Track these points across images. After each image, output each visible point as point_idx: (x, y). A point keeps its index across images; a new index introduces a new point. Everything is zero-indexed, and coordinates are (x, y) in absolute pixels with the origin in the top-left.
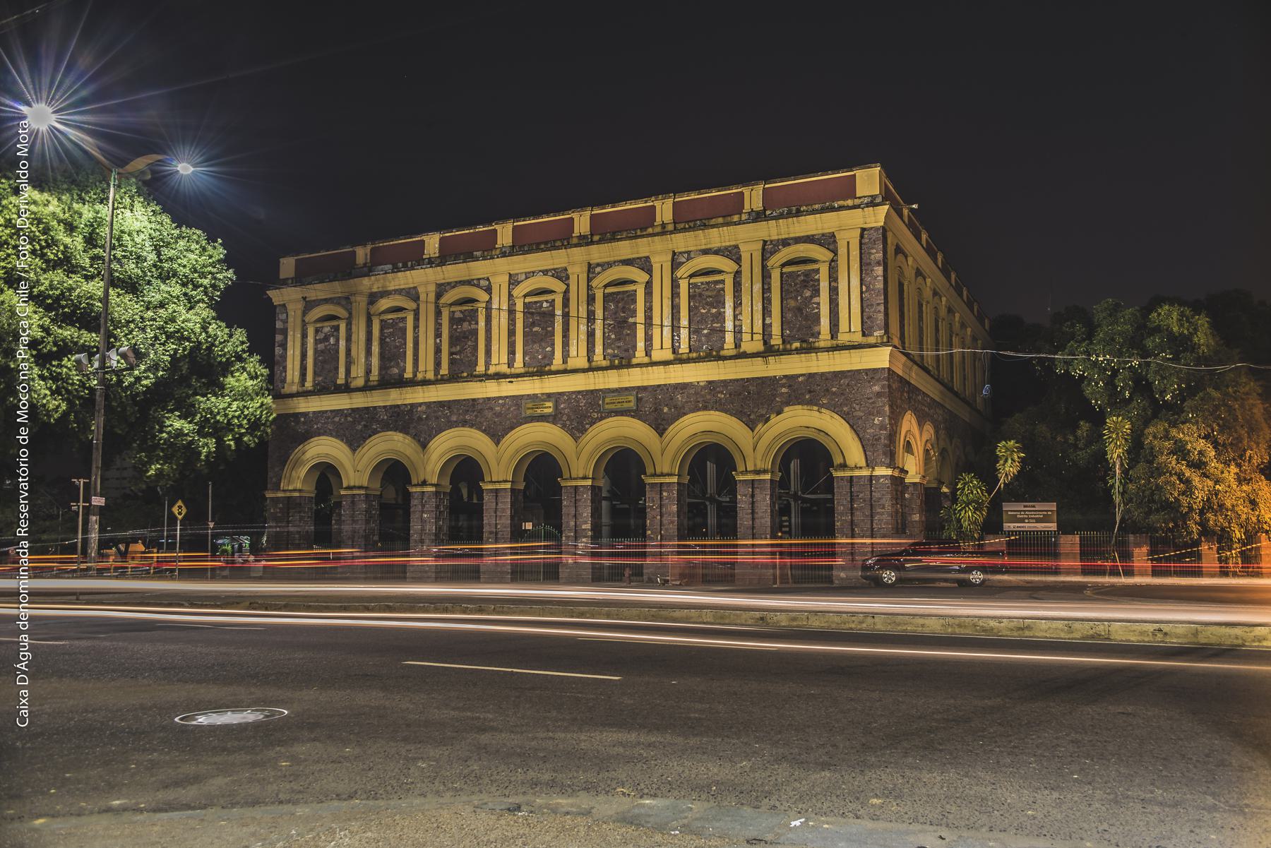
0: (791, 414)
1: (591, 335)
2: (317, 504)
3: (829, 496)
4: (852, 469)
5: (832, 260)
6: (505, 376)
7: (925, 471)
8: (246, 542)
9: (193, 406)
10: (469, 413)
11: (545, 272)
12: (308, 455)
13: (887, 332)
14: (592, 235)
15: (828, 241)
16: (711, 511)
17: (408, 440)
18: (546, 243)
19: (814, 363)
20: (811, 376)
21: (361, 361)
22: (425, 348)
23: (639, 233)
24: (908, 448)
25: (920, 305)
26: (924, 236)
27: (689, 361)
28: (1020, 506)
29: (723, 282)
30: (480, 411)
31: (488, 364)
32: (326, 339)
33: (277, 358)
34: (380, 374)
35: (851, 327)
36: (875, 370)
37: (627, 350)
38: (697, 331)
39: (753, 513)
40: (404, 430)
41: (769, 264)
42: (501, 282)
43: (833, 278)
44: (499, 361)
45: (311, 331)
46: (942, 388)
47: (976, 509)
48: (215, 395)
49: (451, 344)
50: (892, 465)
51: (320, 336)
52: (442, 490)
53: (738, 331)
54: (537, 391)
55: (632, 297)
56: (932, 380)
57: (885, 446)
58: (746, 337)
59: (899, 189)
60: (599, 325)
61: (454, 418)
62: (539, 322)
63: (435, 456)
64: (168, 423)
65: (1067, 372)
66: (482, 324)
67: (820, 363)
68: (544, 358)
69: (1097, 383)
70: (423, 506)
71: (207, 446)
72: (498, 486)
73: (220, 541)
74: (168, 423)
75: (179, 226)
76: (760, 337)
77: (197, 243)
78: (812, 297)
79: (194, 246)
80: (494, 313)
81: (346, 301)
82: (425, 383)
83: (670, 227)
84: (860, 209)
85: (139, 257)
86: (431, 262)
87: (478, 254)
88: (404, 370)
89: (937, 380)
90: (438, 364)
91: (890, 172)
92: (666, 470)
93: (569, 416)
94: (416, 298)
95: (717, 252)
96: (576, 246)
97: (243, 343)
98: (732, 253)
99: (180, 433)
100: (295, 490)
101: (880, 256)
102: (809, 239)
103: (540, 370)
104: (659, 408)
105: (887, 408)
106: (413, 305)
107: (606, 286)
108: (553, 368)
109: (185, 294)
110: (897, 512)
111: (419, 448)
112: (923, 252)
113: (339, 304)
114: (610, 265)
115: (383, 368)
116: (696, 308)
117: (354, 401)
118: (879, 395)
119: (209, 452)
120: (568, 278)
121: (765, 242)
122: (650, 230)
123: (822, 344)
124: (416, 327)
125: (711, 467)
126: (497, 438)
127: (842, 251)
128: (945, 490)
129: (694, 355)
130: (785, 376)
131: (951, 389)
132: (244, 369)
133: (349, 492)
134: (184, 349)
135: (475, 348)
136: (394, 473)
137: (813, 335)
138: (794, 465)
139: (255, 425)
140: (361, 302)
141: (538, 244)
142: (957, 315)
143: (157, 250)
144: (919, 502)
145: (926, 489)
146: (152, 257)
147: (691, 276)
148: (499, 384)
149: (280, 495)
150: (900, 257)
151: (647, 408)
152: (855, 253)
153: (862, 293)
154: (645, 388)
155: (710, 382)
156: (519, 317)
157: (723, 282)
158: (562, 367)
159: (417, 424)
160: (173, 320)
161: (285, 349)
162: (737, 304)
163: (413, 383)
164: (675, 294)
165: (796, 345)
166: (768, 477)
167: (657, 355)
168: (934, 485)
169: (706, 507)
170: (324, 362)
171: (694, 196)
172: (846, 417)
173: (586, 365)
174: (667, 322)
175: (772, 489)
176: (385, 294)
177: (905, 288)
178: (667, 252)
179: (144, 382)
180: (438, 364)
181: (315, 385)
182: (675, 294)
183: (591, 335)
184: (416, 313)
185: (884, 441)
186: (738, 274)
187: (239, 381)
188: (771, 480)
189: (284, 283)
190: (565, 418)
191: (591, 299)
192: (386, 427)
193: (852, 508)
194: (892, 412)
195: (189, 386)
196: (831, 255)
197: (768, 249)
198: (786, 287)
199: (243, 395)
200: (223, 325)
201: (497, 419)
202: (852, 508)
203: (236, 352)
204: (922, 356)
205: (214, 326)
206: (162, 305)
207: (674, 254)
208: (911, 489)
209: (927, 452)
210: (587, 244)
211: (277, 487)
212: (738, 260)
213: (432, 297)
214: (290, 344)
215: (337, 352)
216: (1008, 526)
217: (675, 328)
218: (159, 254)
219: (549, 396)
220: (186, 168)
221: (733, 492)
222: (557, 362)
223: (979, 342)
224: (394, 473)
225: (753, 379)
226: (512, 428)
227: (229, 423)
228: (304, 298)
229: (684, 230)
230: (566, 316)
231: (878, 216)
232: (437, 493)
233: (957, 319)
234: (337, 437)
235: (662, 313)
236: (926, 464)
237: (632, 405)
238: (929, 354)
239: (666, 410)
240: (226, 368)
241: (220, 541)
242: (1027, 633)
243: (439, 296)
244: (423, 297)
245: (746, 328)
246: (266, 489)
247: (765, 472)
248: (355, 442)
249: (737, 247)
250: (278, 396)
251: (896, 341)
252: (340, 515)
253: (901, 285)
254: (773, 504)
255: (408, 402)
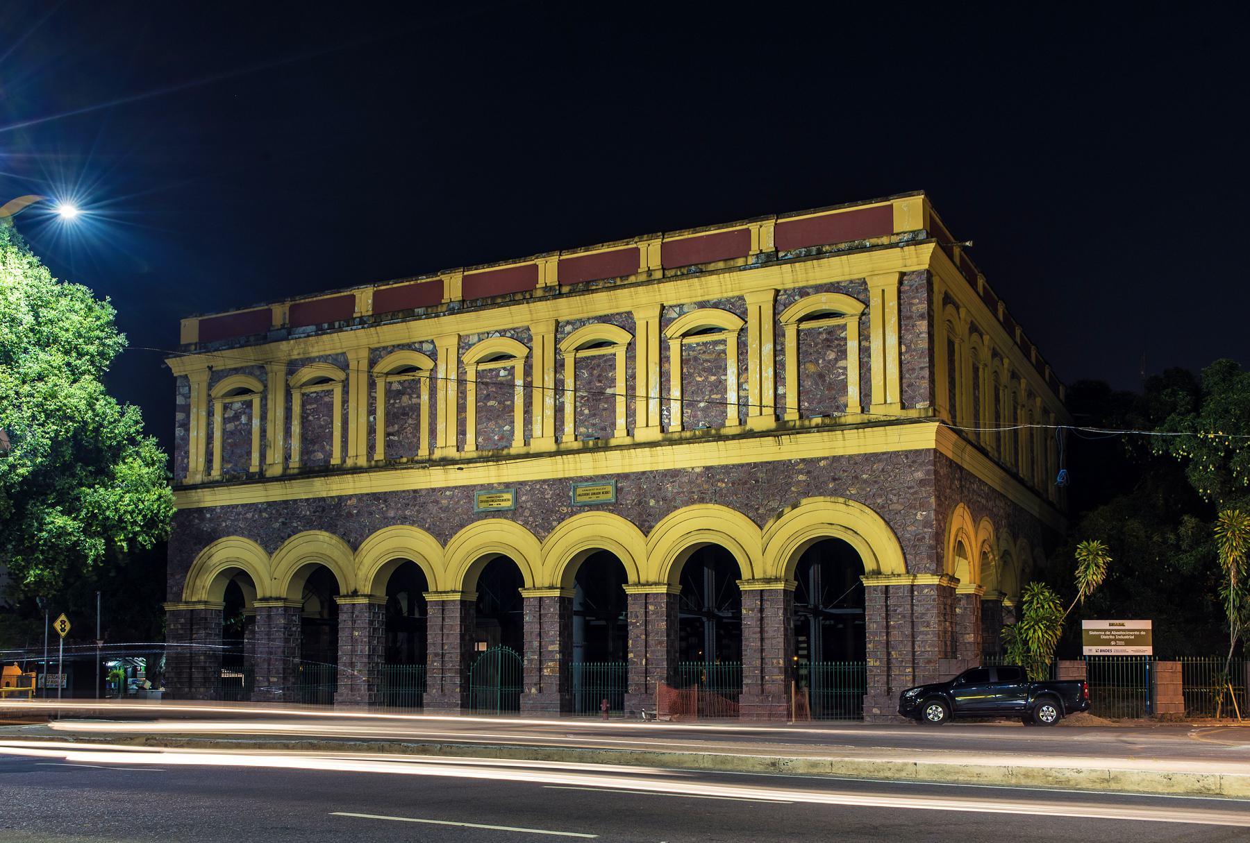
0: (809, 507)
1: (559, 410)
2: (225, 620)
3: (858, 611)
4: (888, 577)
5: (863, 314)
6: (453, 462)
7: (982, 580)
8: (141, 663)
9: (78, 499)
10: (410, 508)
11: (502, 333)
12: (215, 559)
13: (932, 403)
14: (560, 285)
15: (857, 290)
16: (709, 631)
17: (335, 540)
18: (503, 296)
19: (840, 443)
20: (836, 459)
21: (278, 445)
22: (356, 428)
23: (619, 282)
24: (960, 549)
25: (976, 370)
26: (981, 282)
27: (680, 441)
28: (1103, 624)
29: (724, 342)
30: (423, 505)
31: (432, 447)
32: (236, 417)
33: (178, 441)
34: (301, 460)
35: (886, 398)
36: (917, 453)
37: (604, 429)
38: (692, 404)
39: (762, 632)
40: (331, 528)
41: (783, 319)
42: (448, 345)
43: (864, 336)
44: (446, 444)
45: (218, 408)
46: (1004, 474)
47: (1047, 627)
48: (104, 486)
49: (388, 423)
50: (939, 571)
51: (230, 414)
52: (376, 602)
53: (742, 404)
54: (493, 480)
55: (610, 362)
56: (990, 464)
57: (931, 547)
58: (754, 411)
59: (942, 227)
60: (568, 398)
61: (391, 514)
62: (495, 394)
63: (368, 561)
64: (48, 519)
65: (1167, 453)
66: (425, 397)
67: (847, 443)
68: (501, 439)
69: (1206, 468)
70: (354, 622)
71: (95, 548)
72: (444, 597)
73: (111, 664)
74: (48, 519)
75: (60, 282)
76: (771, 411)
77: (82, 301)
78: (836, 360)
79: (78, 306)
80: (440, 384)
81: (260, 371)
82: (356, 470)
83: (658, 275)
84: (892, 257)
85: (13, 320)
86: (363, 322)
87: (420, 311)
88: (331, 455)
89: (997, 464)
90: (371, 448)
91: (935, 202)
92: (652, 579)
93: (532, 511)
94: (345, 367)
95: (716, 305)
96: (541, 299)
97: (137, 422)
98: (736, 306)
99: (62, 532)
100: (199, 602)
101: (923, 307)
102: (834, 288)
103: (497, 455)
104: (643, 500)
105: (933, 500)
106: (340, 375)
107: (577, 349)
108: (513, 451)
109: (68, 364)
110: (945, 632)
111: (349, 551)
112: (978, 301)
113: (251, 374)
114: (582, 322)
115: (305, 452)
116: (691, 375)
117: (270, 492)
118: (922, 483)
119: (98, 555)
120: (531, 339)
121: (777, 292)
122: (632, 279)
123: (849, 419)
124: (345, 402)
125: (709, 575)
126: (443, 536)
127: (875, 301)
128: (1007, 603)
129: (688, 434)
130: (803, 460)
131: (1015, 476)
132: (138, 453)
133: (265, 605)
134: (67, 432)
135: (417, 427)
136: (319, 580)
137: (838, 408)
138: (814, 572)
139: (151, 522)
140: (279, 370)
141: (494, 298)
142: (1023, 381)
143: (34, 309)
144: (973, 619)
145: (983, 602)
146: (29, 320)
147: (684, 335)
148: (446, 471)
149: (182, 607)
150: (950, 308)
151: (629, 500)
152: (892, 304)
153: (900, 354)
154: (625, 476)
155: (708, 468)
156: (471, 388)
157: (724, 342)
158: (523, 450)
159: (348, 520)
160: (54, 396)
161: (187, 430)
162: (742, 370)
163: (341, 471)
164: (663, 359)
165: (817, 420)
166: (781, 586)
167: (641, 435)
168: (993, 598)
169: (702, 624)
170: (234, 445)
171: (687, 235)
172: (880, 511)
173: (553, 448)
174: (654, 392)
175: (786, 602)
176: (308, 361)
177: (956, 346)
178: (656, 304)
179: (21, 471)
180: (371, 448)
181: (223, 473)
182: (663, 359)
183: (559, 410)
184: (346, 385)
185: (929, 541)
186: (743, 331)
187: (131, 468)
188: (785, 591)
189: (186, 349)
190: (527, 513)
191: (559, 366)
192: (310, 525)
193: (888, 627)
194: (939, 505)
195: (73, 475)
196: (861, 307)
197: (780, 300)
198: (803, 348)
199: (137, 486)
200: (113, 401)
201: (444, 515)
202: (888, 627)
203: (129, 434)
204: (978, 434)
205: (102, 402)
206: (40, 378)
207: (663, 307)
208: (963, 602)
209: (984, 555)
210: (555, 297)
211: (178, 598)
212: (743, 316)
213: (364, 365)
214: (193, 424)
215: (250, 432)
216: (1088, 650)
217: (664, 400)
218: (37, 316)
219: (508, 486)
220: (68, 212)
221: (737, 605)
222: (517, 446)
223: (1052, 415)
224: (319, 580)
225: (762, 463)
226: (462, 526)
227: (121, 520)
228: (210, 368)
229: (675, 278)
230: (528, 386)
231: (921, 257)
232: (370, 606)
233: (1023, 385)
234: (250, 536)
235: (647, 382)
236: (982, 571)
237: (610, 497)
238: (987, 431)
239: (652, 503)
240: (117, 454)
241: (111, 664)
242: (1113, 786)
243: (372, 363)
244: (353, 365)
245: (753, 400)
246: (165, 600)
247: (777, 580)
248: (271, 542)
249: (741, 298)
250: (179, 488)
251: (945, 415)
252: (253, 632)
253: (951, 344)
254: (786, 620)
255: (334, 494)
